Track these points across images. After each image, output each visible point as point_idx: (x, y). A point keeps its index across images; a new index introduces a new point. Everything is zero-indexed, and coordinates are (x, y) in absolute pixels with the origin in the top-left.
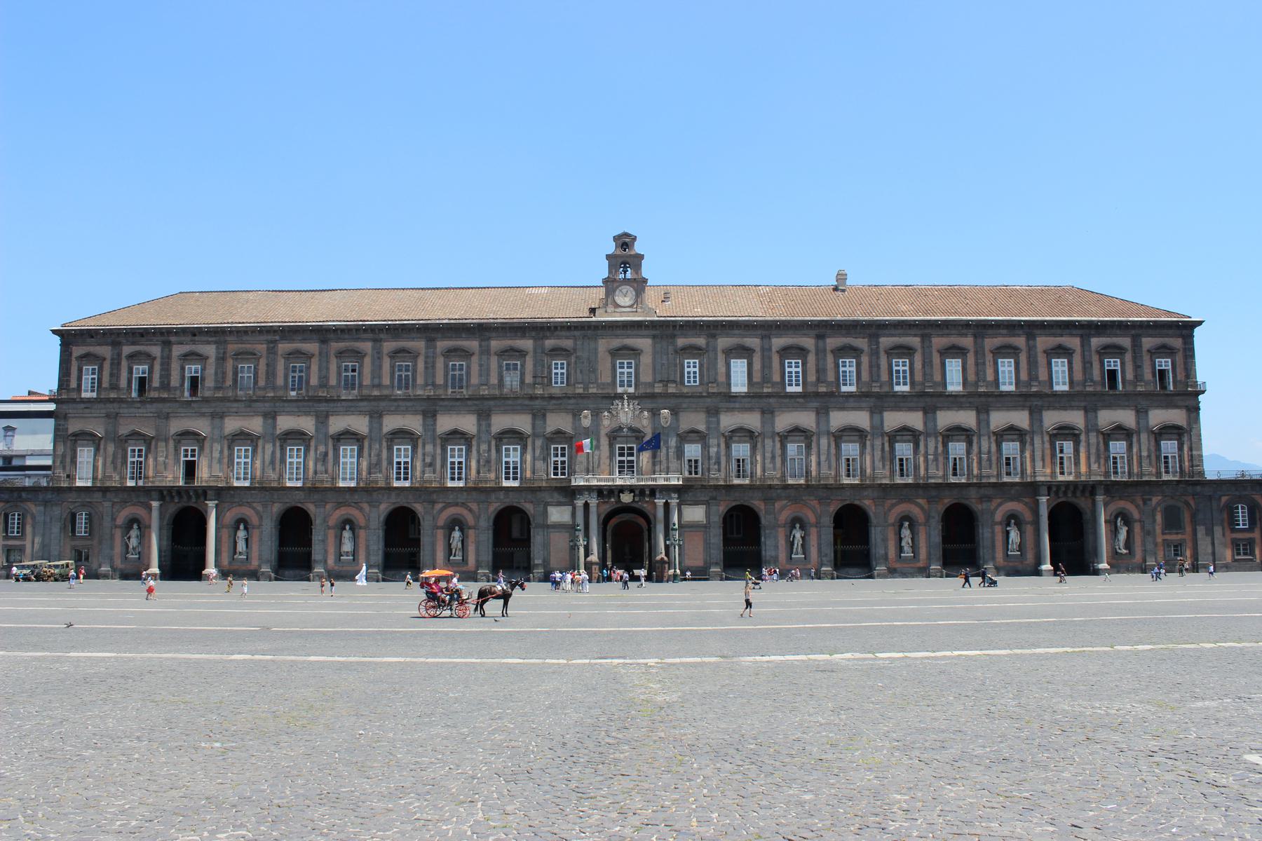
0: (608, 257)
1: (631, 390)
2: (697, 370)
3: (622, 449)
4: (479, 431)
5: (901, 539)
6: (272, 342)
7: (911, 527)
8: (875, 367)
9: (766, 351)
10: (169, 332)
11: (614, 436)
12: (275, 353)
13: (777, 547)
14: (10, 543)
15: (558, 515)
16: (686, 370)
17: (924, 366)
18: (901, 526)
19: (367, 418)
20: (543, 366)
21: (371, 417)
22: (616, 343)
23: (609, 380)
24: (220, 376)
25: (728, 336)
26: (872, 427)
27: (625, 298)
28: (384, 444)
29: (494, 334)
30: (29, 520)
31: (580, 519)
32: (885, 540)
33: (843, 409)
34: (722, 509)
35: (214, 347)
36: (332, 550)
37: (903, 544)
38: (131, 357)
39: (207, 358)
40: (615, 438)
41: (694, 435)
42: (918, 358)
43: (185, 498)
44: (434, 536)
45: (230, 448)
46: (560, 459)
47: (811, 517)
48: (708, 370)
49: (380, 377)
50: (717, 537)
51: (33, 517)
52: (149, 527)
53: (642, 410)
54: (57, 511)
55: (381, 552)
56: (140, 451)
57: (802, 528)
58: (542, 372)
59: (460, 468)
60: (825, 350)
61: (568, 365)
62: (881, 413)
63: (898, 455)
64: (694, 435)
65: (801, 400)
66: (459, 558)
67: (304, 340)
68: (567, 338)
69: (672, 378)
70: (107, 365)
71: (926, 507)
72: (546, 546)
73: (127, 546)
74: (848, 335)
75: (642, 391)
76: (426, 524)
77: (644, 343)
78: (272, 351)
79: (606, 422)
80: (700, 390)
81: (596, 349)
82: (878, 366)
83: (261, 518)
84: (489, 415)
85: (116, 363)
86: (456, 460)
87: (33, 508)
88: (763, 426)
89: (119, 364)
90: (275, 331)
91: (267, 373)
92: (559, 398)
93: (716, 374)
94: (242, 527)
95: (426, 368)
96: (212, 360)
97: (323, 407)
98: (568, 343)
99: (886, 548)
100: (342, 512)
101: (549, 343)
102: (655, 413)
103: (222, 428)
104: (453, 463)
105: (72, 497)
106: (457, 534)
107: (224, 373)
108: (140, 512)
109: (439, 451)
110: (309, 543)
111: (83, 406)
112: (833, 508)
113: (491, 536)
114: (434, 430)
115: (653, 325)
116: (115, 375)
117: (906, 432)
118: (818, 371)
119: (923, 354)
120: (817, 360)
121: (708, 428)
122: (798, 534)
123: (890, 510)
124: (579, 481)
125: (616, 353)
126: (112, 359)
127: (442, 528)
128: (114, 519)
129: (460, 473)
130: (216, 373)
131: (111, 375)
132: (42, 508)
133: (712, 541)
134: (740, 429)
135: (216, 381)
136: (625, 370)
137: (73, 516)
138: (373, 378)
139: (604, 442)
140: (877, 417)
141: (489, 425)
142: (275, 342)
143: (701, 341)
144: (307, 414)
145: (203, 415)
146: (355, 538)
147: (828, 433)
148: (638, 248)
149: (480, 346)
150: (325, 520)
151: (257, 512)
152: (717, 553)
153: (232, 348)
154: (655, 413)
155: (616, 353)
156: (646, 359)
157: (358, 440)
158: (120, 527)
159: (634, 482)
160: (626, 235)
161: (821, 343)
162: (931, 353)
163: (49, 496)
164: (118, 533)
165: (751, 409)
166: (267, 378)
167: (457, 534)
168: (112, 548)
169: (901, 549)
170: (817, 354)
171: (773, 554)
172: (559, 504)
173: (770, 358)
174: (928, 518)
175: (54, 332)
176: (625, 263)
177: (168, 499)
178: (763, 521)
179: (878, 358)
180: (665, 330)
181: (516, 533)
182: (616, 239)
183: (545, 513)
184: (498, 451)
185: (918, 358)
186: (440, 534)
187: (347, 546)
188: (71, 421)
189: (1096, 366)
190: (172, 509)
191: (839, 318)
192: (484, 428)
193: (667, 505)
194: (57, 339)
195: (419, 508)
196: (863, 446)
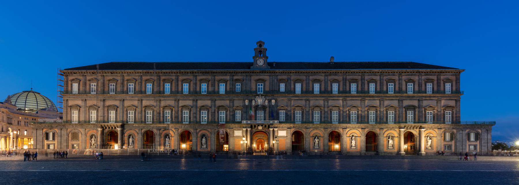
0: (255, 49)
23: (255, 90)
27: (261, 62)
53: (266, 99)
57: (318, 138)
66: (205, 147)
77: (266, 77)
79: (253, 103)
101: (235, 78)
106: (204, 140)
125: (258, 81)
136: (261, 86)
148: (264, 47)
150: (160, 134)
154: (270, 101)
156: (267, 83)
167: (204, 140)
182: (257, 43)
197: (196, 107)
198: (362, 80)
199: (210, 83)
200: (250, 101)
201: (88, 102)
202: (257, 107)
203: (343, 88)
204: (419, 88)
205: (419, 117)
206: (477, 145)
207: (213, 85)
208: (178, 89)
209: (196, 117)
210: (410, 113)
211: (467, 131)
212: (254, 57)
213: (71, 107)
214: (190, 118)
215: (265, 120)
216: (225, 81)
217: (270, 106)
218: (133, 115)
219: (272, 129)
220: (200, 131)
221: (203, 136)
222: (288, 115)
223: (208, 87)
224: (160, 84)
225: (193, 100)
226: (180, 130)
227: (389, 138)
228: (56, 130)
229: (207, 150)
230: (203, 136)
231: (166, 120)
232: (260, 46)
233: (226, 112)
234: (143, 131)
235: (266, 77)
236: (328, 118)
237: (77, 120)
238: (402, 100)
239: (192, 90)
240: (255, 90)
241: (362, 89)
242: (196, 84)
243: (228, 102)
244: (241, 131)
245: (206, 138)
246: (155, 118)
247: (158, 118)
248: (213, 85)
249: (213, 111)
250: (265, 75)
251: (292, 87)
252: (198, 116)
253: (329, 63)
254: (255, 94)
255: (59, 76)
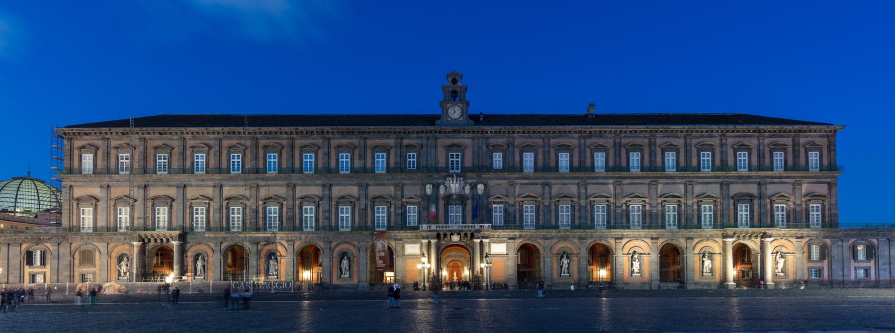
23: (444, 165)
66: (347, 275)
77: (465, 140)
79: (442, 191)
109: (333, 210)
150: (258, 252)
154: (474, 187)
167: (345, 262)
189: (767, 156)
197: (330, 199)
198: (650, 145)
199: (357, 152)
200: (436, 187)
201: (113, 190)
202: (448, 198)
203: (615, 162)
204: (759, 161)
205: (760, 214)
206: (870, 268)
207: (363, 157)
208: (293, 164)
209: (329, 218)
210: (744, 208)
211: (852, 240)
212: (441, 104)
213: (78, 199)
214: (317, 220)
215: (464, 222)
216: (387, 149)
217: (475, 197)
218: (204, 216)
219: (479, 241)
220: (337, 245)
221: (343, 255)
222: (509, 214)
223: (352, 159)
224: (257, 154)
225: (324, 186)
226: (298, 244)
227: (703, 257)
228: (48, 245)
229: (351, 282)
230: (343, 255)
231: (270, 224)
233: (389, 208)
234: (224, 246)
235: (466, 140)
238: (728, 184)
239: (320, 165)
240: (444, 165)
241: (651, 162)
242: (328, 154)
243: (392, 188)
244: (418, 246)
245: (349, 259)
246: (248, 222)
247: (254, 220)
248: (363, 157)
249: (363, 206)
251: (517, 159)
252: (333, 216)
253: (587, 116)
254: (445, 173)
255: (55, 139)
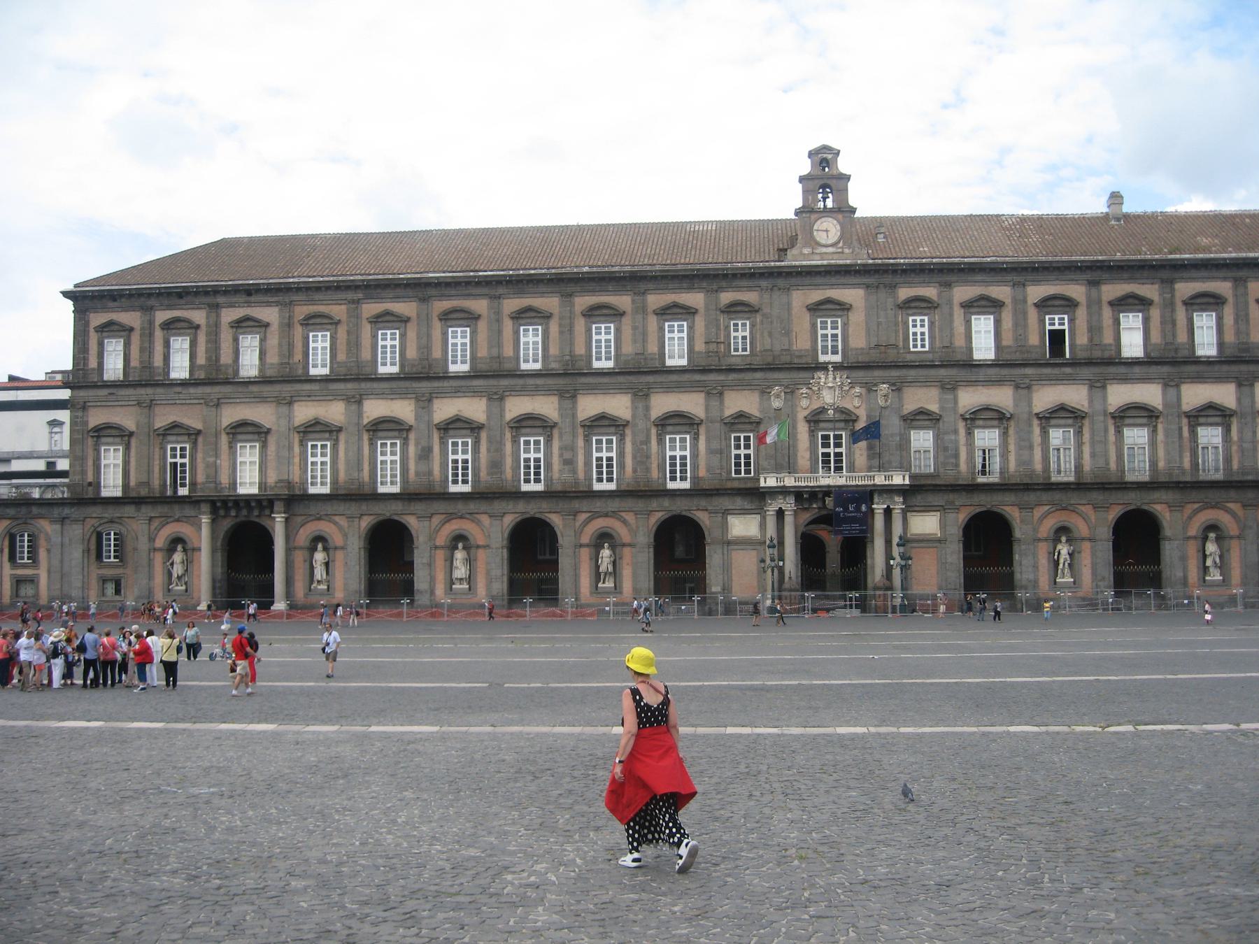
0: (802, 179)
1: (837, 358)
2: (926, 330)
3: (826, 437)
4: (634, 416)
5: (1205, 557)
6: (353, 302)
7: (1219, 539)
8: (1169, 323)
9: (1020, 303)
10: (216, 291)
11: (815, 419)
12: (358, 317)
13: (1036, 567)
14: (20, 572)
15: (743, 526)
16: (912, 330)
17: (1236, 321)
18: (1205, 539)
19: (484, 400)
20: (718, 329)
21: (490, 399)
22: (817, 295)
24: (285, 348)
25: (966, 283)
26: (1165, 405)
28: (508, 435)
29: (651, 286)
30: (42, 543)
31: (771, 531)
32: (1184, 558)
33: (1125, 380)
34: (962, 517)
35: (276, 310)
36: (440, 576)
37: (1209, 562)
38: (169, 326)
39: (267, 325)
40: (817, 422)
41: (921, 418)
42: (1228, 312)
43: (244, 512)
44: (576, 556)
45: (302, 444)
46: (742, 452)
47: (1081, 528)
48: (941, 330)
49: (500, 345)
50: (954, 554)
51: (48, 539)
52: (199, 549)
54: (76, 531)
55: (505, 579)
56: (182, 449)
58: (717, 335)
59: (610, 466)
60: (1100, 302)
61: (752, 326)
62: (1178, 386)
63: (1202, 441)
64: (921, 418)
65: (1068, 370)
66: (609, 584)
67: (397, 298)
68: (750, 289)
69: (892, 341)
70: (135, 339)
71: (1240, 512)
72: (727, 568)
73: (170, 574)
74: (1132, 279)
75: (852, 359)
76: (565, 541)
77: (852, 295)
78: (355, 315)
79: (804, 403)
80: (930, 356)
81: (789, 304)
82: (1174, 323)
83: (345, 536)
84: (647, 396)
85: (148, 334)
86: (604, 455)
87: (47, 527)
88: (1016, 405)
89: (151, 335)
90: (357, 287)
91: (348, 343)
92: (741, 370)
93: (952, 335)
94: (320, 546)
95: (561, 333)
96: (275, 327)
97: (425, 386)
98: (751, 297)
99: (1185, 570)
100: (455, 526)
101: (726, 297)
102: (870, 388)
103: (290, 418)
104: (599, 459)
105: (96, 511)
107: (291, 346)
108: (184, 529)
110: (409, 567)
111: (105, 392)
112: (1113, 514)
113: (652, 555)
114: (574, 416)
115: (865, 271)
116: (147, 350)
117: (1212, 413)
118: (1090, 329)
119: (1236, 305)
120: (1090, 314)
121: (942, 408)
122: (1064, 549)
123: (1190, 518)
124: (769, 481)
125: (815, 309)
126: (142, 329)
127: (587, 546)
128: (152, 539)
129: (610, 473)
130: (280, 345)
131: (142, 350)
132: (58, 527)
133: (949, 560)
134: (987, 409)
135: (281, 355)
136: (829, 329)
137: (99, 536)
138: (490, 347)
139: (803, 429)
140: (1172, 392)
141: (647, 408)
142: (358, 302)
143: (930, 292)
144: (403, 395)
145: (263, 399)
146: (470, 561)
147: (1105, 413)
148: (843, 166)
149: (633, 301)
150: (432, 538)
151: (340, 528)
152: (956, 576)
153: (301, 311)
154: (870, 388)
155: (815, 309)
157: (472, 429)
158: (160, 550)
159: (841, 481)
160: (825, 148)
161: (1094, 291)
162: (1247, 303)
163: (67, 511)
164: (158, 558)
165: (999, 382)
166: (349, 351)
167: (606, 553)
168: (151, 577)
169: (1205, 569)
170: (1089, 307)
171: (1031, 577)
172: (744, 512)
173: (1025, 313)
174: (1243, 528)
175: (66, 294)
176: (824, 187)
177: (222, 512)
178: (1017, 533)
179: (1173, 311)
180: (879, 275)
181: (680, 552)
183: (725, 526)
184: (661, 441)
185: (1228, 312)
186: (585, 553)
187: (461, 571)
188: (92, 412)
190: (226, 524)
191: (1118, 256)
192: (640, 411)
193: (888, 512)
194: (69, 305)
195: (556, 520)
196: (1154, 431)
209: (569, 462)
221: (604, 538)
222: (946, 449)
232: (824, 163)
236: (1106, 455)
237: (120, 482)
250: (845, 285)
